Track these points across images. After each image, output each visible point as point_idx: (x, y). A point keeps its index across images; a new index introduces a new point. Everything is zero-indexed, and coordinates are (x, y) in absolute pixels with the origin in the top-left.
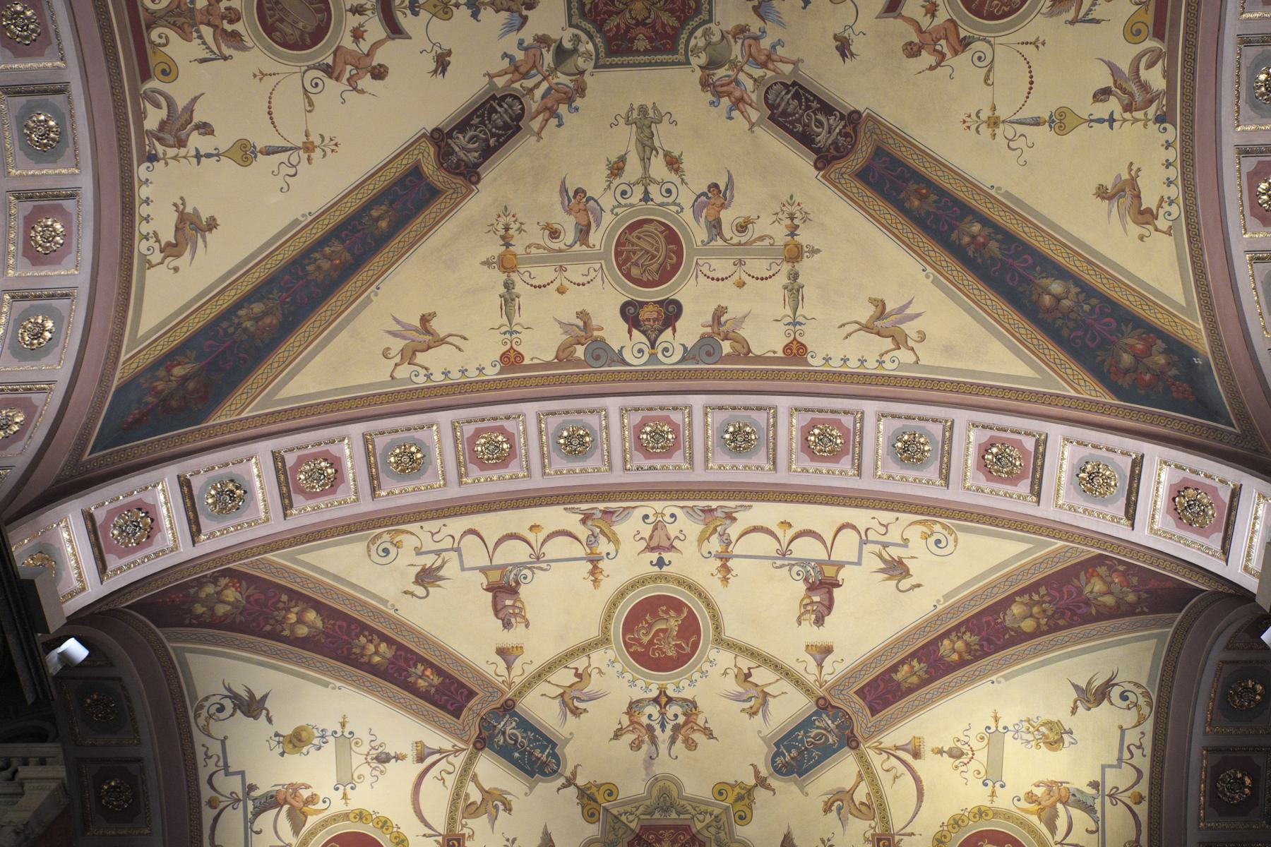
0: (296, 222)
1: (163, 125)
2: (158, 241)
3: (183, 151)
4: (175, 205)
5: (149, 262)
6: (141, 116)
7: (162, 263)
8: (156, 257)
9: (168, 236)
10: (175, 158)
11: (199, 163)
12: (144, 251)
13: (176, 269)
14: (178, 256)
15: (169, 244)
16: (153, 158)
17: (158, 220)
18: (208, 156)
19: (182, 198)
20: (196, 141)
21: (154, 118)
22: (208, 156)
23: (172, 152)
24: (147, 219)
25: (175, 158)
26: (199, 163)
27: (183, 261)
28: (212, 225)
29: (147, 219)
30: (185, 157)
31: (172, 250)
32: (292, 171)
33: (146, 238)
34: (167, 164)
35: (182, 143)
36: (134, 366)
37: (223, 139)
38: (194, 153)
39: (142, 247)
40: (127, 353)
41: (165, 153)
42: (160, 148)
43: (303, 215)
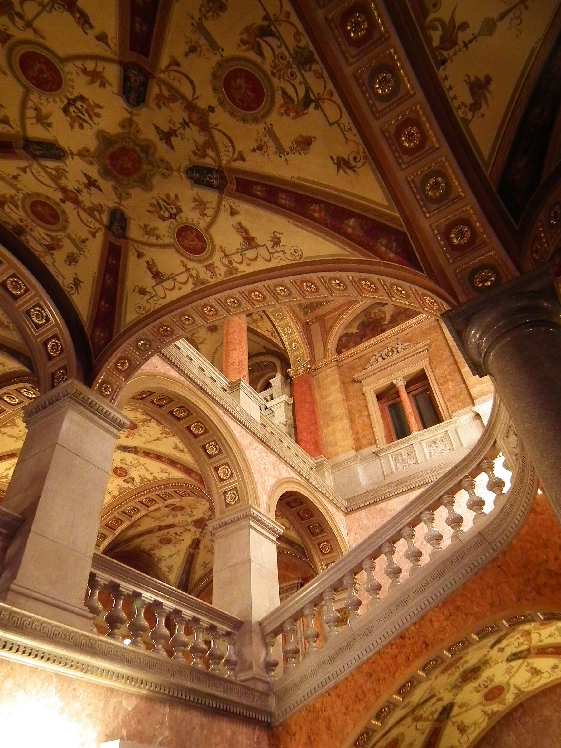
0: (533, 50)
1: (442, 39)
2: (466, 106)
3: (457, 48)
4: (465, 81)
5: (467, 120)
6: (429, 40)
7: (474, 117)
8: (469, 115)
9: (469, 100)
10: (455, 54)
11: (467, 49)
12: (462, 116)
13: (483, 116)
14: (480, 108)
15: (472, 105)
16: (444, 62)
17: (459, 94)
18: (471, 41)
19: (467, 75)
20: (462, 37)
21: (436, 37)
22: (471, 41)
23: (452, 52)
24: (455, 98)
25: (455, 54)
26: (467, 49)
27: (484, 109)
28: (488, 79)
29: (455, 98)
30: (460, 50)
31: (475, 107)
32: (518, 21)
33: (459, 108)
34: (452, 61)
35: (454, 43)
36: (495, 175)
37: (475, 27)
38: (462, 44)
39: (460, 114)
40: (487, 170)
41: (449, 55)
42: (445, 53)
43: (536, 43)
